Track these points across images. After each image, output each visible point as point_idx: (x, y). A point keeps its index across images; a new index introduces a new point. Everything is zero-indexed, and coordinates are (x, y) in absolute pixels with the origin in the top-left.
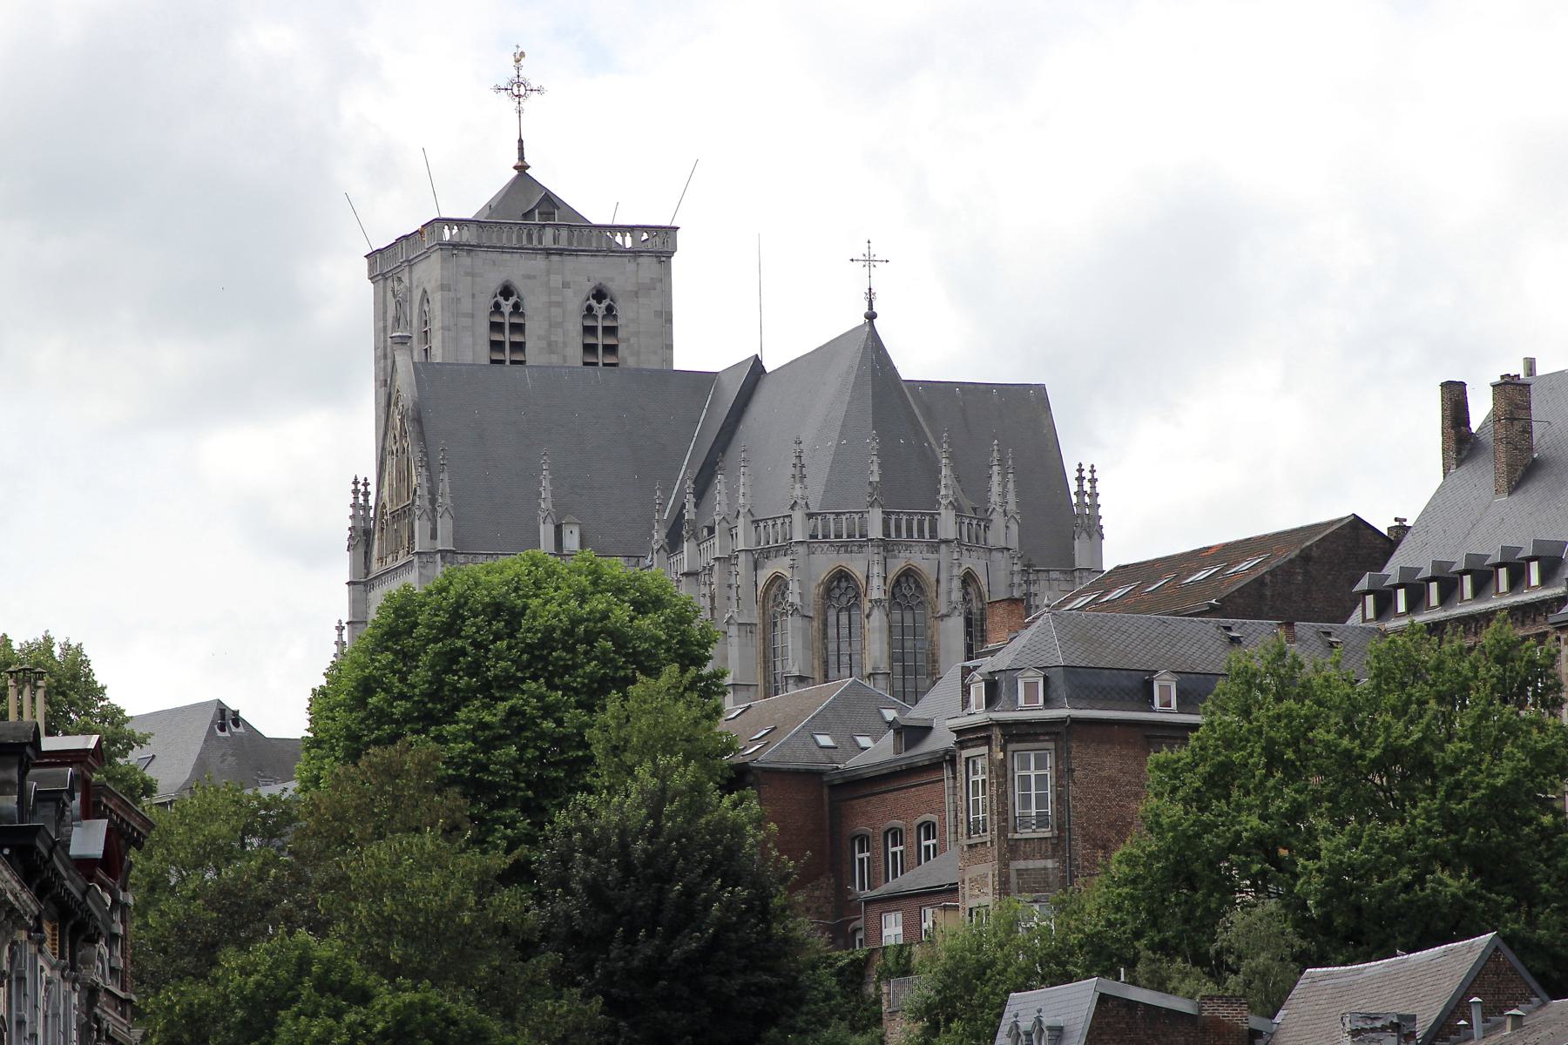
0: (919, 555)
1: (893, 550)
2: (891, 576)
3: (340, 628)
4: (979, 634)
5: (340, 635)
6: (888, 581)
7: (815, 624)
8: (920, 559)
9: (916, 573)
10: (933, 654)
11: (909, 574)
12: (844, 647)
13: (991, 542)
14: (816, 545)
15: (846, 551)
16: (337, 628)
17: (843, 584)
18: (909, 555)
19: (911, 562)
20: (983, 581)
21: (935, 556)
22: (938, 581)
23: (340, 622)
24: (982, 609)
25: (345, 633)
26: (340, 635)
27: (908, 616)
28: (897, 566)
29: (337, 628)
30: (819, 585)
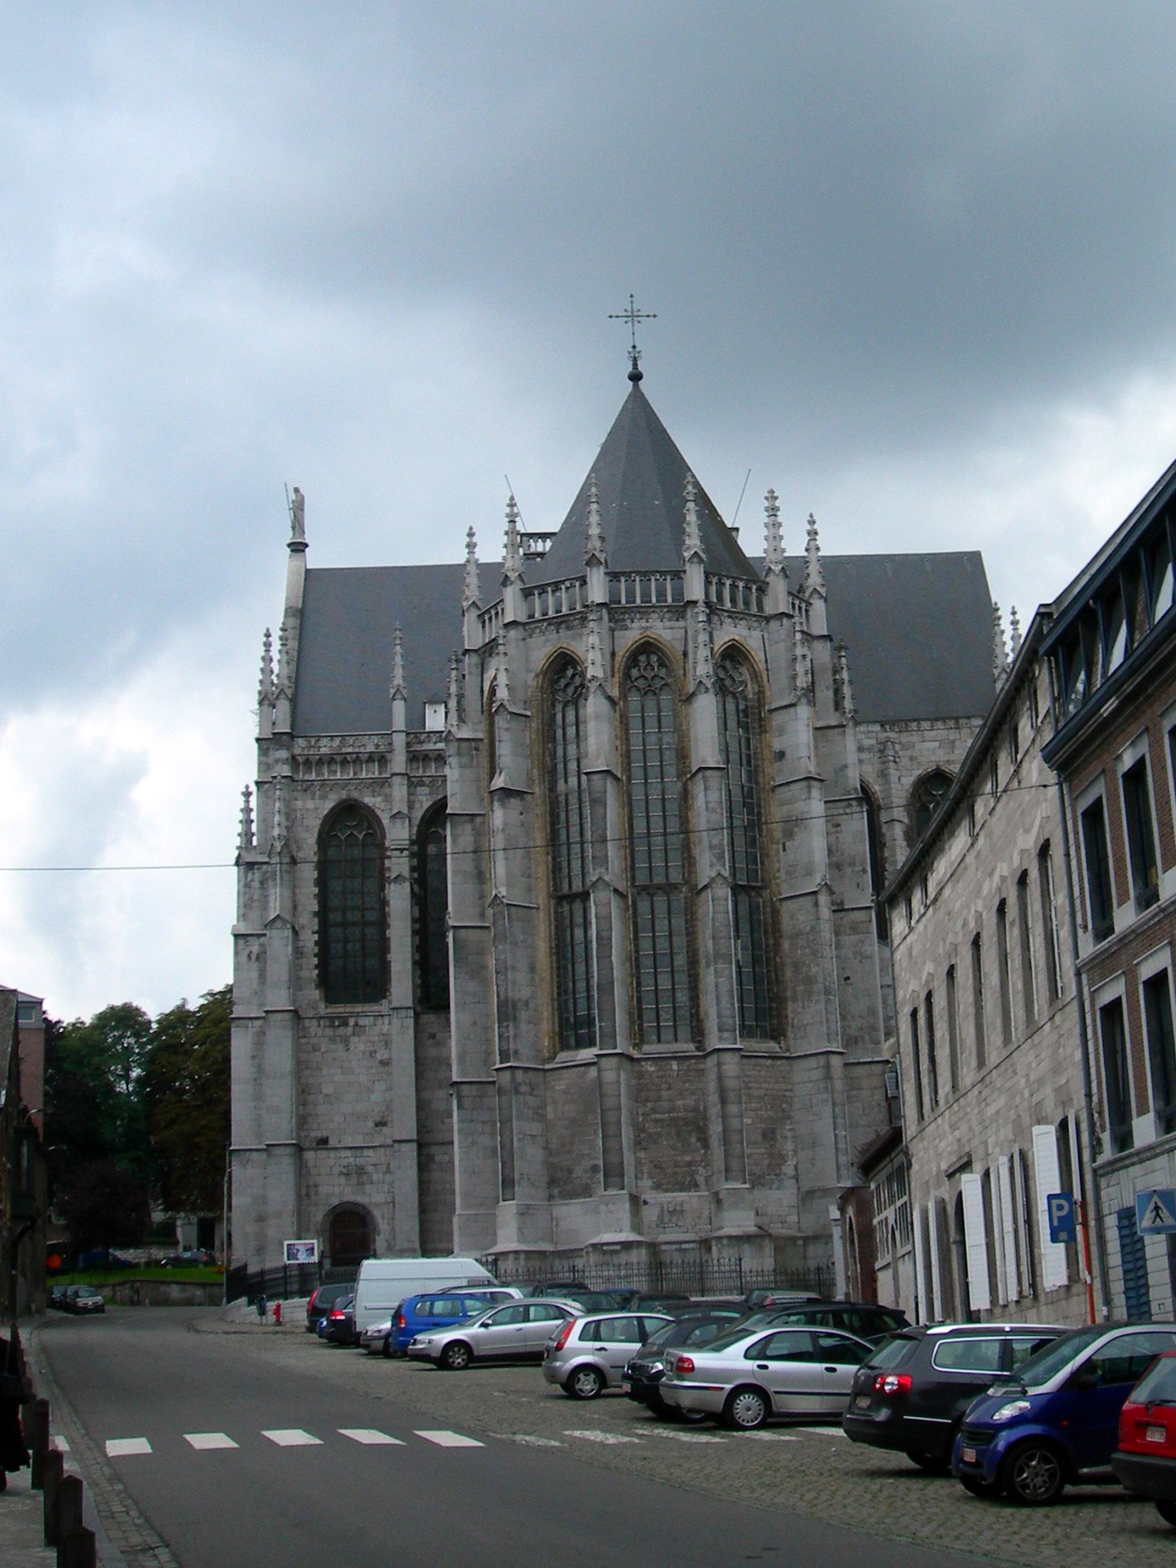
0: (659, 624)
1: (624, 620)
2: (621, 653)
3: (247, 794)
4: (757, 726)
5: (247, 802)
6: (618, 659)
7: (534, 725)
8: (663, 630)
9: (660, 649)
10: (683, 748)
11: (647, 647)
12: (572, 749)
13: (769, 610)
14: (532, 626)
15: (568, 628)
16: (243, 794)
17: (570, 672)
18: (644, 624)
19: (649, 633)
20: (758, 656)
21: (682, 623)
22: (685, 654)
23: (247, 787)
24: (759, 692)
25: (253, 802)
26: (247, 802)
27: (650, 703)
28: (631, 636)
29: (243, 794)
30: (537, 676)
